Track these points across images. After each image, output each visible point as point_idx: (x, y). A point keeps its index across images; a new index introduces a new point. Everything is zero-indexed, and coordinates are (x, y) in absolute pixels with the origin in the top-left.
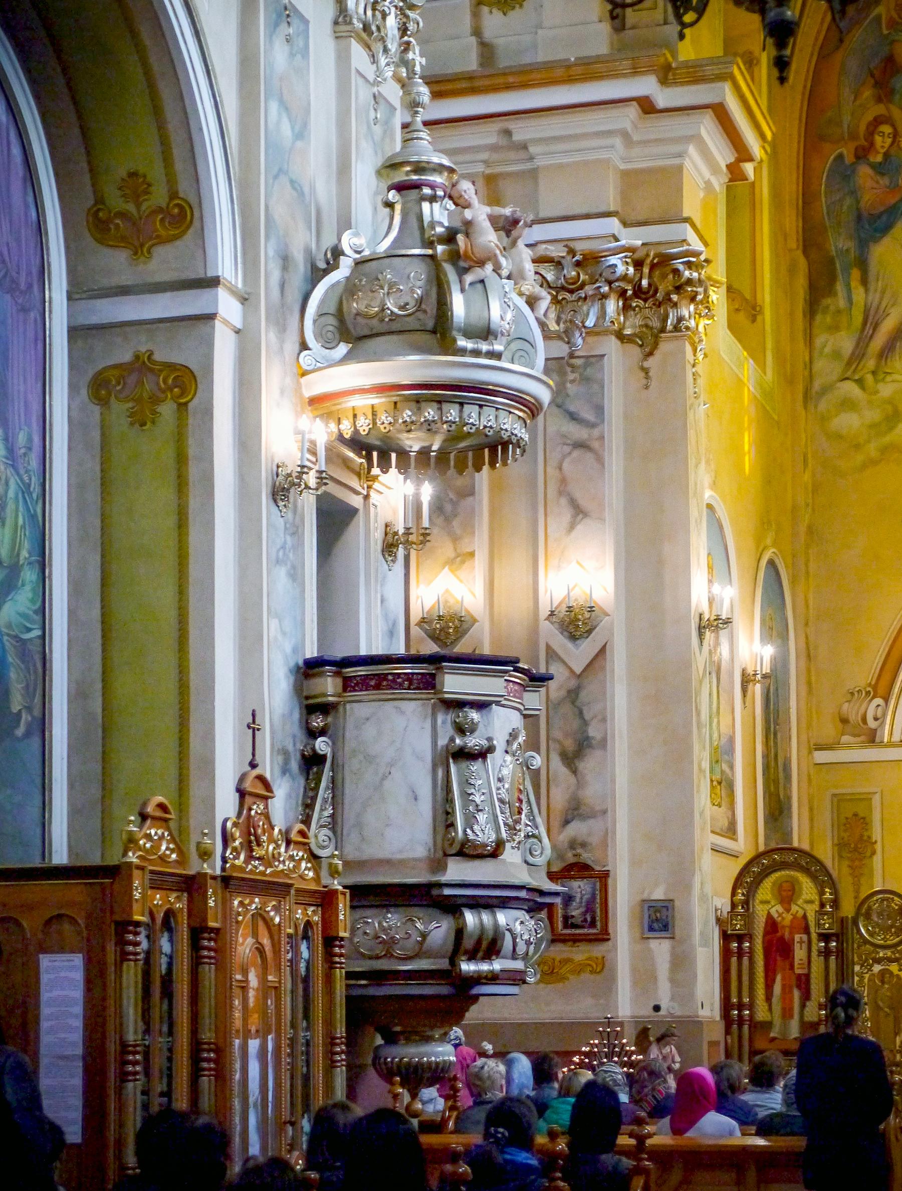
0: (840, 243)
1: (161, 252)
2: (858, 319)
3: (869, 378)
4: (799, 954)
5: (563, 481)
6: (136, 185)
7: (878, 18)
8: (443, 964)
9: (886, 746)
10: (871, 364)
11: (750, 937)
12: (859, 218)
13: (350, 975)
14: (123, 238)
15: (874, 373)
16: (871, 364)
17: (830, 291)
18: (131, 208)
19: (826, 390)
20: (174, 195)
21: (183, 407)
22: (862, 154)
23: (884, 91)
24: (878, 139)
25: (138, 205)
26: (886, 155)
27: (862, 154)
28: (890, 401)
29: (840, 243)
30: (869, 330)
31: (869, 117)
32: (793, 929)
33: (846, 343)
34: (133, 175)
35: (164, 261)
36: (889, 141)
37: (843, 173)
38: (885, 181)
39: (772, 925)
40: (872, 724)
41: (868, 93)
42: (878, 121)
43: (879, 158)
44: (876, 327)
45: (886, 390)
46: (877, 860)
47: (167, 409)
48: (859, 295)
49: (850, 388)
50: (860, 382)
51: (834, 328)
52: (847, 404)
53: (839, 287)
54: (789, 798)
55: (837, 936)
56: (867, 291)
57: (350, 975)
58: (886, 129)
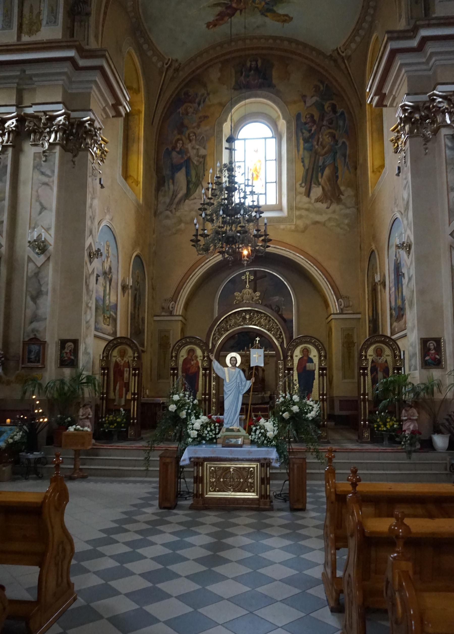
0: (167, 172)
2: (171, 193)
3: (174, 210)
7: (179, 112)
9: (175, 316)
10: (174, 206)
15: (175, 209)
19: (161, 213)
24: (178, 145)
26: (180, 149)
27: (174, 148)
30: (174, 197)
33: (168, 200)
36: (181, 145)
37: (168, 153)
38: (180, 156)
40: (171, 309)
41: (176, 132)
42: (178, 140)
43: (178, 150)
44: (176, 196)
45: (178, 214)
49: (168, 213)
50: (171, 211)
52: (167, 217)
53: (166, 184)
54: (144, 330)
56: (174, 186)
58: (181, 142)
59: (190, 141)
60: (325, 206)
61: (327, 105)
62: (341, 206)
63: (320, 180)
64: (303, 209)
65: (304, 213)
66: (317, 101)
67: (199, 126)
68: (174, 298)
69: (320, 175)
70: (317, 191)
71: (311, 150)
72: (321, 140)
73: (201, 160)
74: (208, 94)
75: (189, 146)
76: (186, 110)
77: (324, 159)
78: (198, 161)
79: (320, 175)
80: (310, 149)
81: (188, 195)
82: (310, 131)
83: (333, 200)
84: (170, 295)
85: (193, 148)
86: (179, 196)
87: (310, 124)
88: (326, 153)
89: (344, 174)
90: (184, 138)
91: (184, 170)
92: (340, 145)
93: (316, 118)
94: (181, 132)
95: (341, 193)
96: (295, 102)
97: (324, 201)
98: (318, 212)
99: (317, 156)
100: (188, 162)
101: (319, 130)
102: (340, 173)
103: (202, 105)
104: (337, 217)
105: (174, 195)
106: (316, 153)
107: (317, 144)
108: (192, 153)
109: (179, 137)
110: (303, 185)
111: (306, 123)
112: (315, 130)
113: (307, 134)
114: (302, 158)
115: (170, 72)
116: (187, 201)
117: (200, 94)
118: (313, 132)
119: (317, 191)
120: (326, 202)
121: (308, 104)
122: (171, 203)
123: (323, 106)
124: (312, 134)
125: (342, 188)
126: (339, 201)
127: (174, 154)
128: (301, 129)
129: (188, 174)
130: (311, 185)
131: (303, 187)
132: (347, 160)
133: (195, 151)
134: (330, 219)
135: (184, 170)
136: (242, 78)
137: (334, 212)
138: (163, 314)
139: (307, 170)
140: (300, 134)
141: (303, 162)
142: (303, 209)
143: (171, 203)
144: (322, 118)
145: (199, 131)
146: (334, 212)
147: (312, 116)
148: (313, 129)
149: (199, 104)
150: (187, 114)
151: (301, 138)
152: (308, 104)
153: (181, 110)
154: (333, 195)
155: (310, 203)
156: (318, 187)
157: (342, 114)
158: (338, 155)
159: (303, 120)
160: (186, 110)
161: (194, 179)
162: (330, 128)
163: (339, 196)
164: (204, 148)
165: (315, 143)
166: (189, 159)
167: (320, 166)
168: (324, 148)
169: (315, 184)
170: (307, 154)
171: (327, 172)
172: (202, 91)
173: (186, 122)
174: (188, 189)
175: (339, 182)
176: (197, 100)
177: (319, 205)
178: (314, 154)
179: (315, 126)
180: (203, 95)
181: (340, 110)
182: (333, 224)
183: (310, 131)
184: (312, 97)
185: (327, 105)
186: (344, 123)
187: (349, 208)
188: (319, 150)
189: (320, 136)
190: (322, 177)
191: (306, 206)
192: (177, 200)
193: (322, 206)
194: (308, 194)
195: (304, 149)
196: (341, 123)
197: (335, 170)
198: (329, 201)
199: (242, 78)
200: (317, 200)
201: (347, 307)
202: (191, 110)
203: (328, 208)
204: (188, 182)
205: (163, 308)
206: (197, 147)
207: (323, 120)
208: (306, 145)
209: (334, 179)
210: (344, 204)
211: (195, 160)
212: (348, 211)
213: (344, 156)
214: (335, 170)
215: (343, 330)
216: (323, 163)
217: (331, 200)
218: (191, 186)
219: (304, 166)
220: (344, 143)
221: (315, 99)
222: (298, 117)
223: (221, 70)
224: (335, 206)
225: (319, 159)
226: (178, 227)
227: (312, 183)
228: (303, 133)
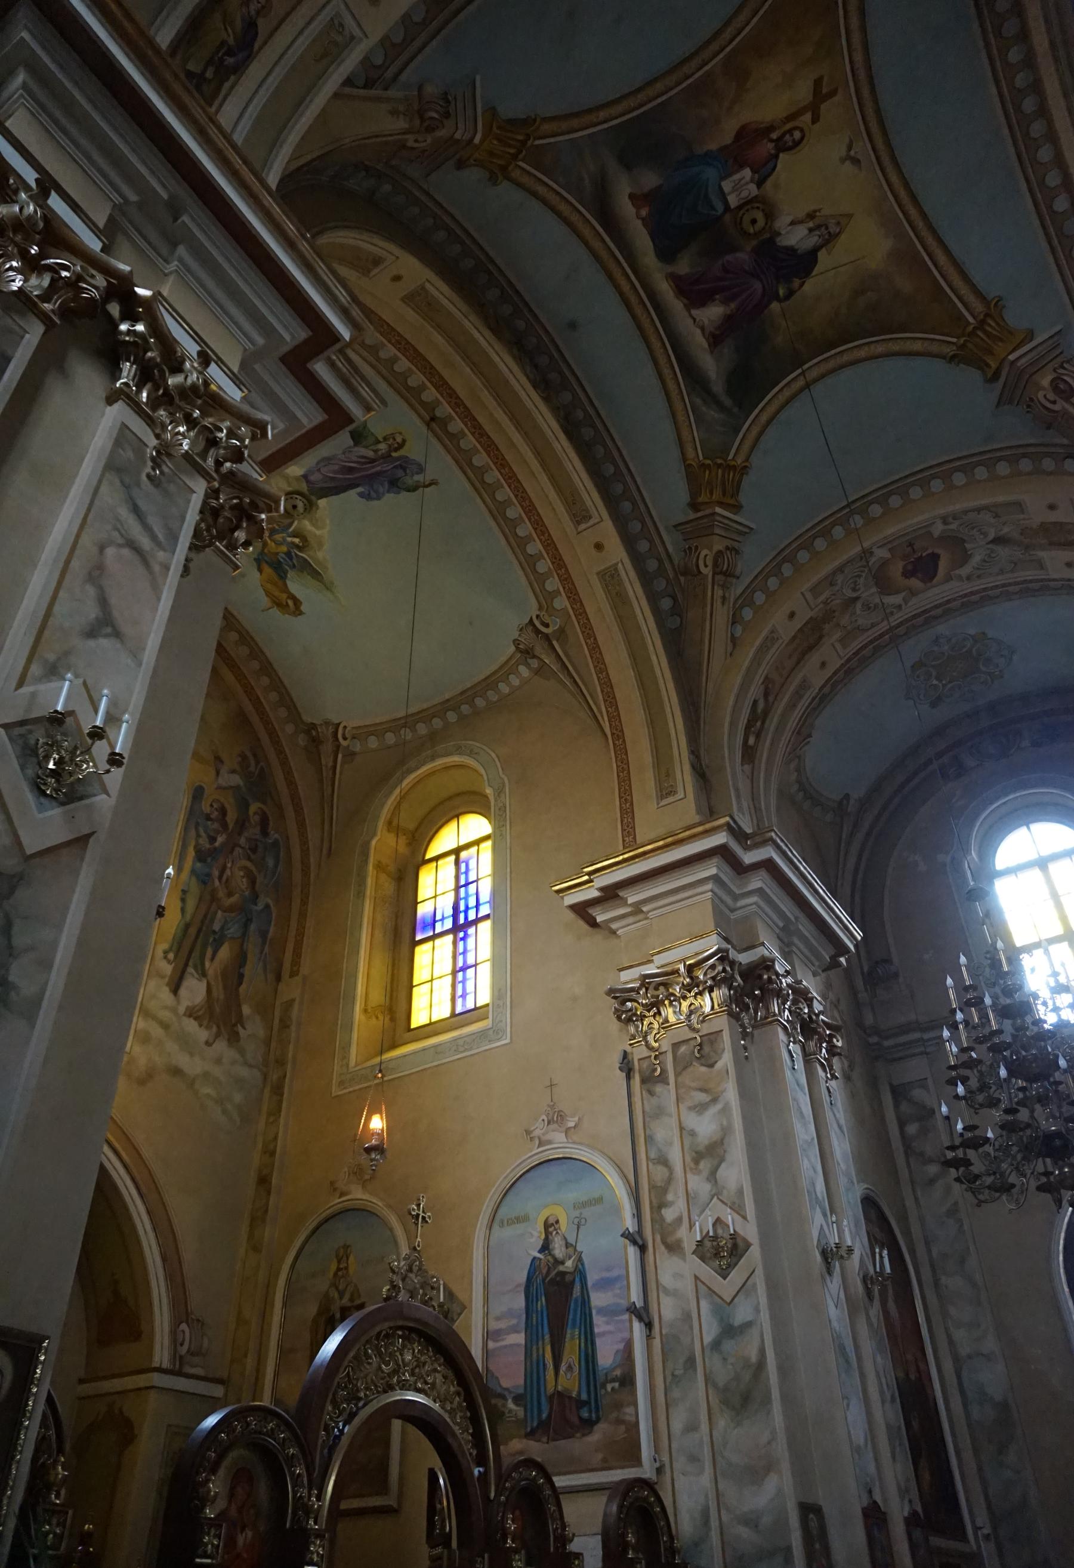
60: (203, 1035)
63: (207, 964)
64: (154, 1018)
65: (157, 1031)
66: (238, 787)
69: (209, 952)
71: (204, 883)
72: (228, 872)
77: (226, 922)
79: (209, 952)
80: (204, 880)
82: (213, 840)
83: (222, 1028)
87: (216, 826)
88: (230, 909)
92: (260, 906)
93: (231, 817)
95: (240, 1020)
97: (205, 1023)
98: (185, 1042)
99: (214, 907)
102: (247, 971)
106: (214, 898)
107: (220, 878)
110: (171, 956)
111: (208, 818)
112: (223, 844)
113: (204, 842)
114: (184, 892)
118: (217, 844)
119: (195, 990)
120: (208, 1028)
121: (221, 781)
124: (215, 849)
125: (246, 1010)
126: (234, 1039)
128: (197, 824)
130: (186, 965)
131: (169, 962)
132: (266, 949)
134: (206, 1075)
137: (218, 1061)
139: (187, 926)
140: (193, 833)
141: (183, 900)
142: (154, 1018)
146: (218, 1061)
147: (223, 811)
148: (220, 840)
151: (193, 843)
152: (221, 781)
154: (222, 1016)
155: (174, 1010)
156: (200, 980)
157: (276, 844)
158: (253, 927)
159: (206, 807)
162: (249, 859)
163: (235, 1025)
165: (216, 873)
167: (214, 932)
168: (230, 895)
169: (195, 968)
170: (195, 888)
171: (225, 952)
175: (242, 989)
179: (224, 836)
181: (274, 836)
182: (207, 1090)
183: (213, 840)
184: (233, 772)
185: (254, 807)
186: (276, 866)
187: (251, 1066)
188: (221, 894)
189: (229, 865)
190: (212, 959)
191: (165, 1015)
195: (193, 871)
196: (270, 862)
197: (241, 959)
198: (215, 1029)
200: (191, 1013)
201: (192, 1354)
203: (208, 1044)
208: (198, 865)
209: (234, 976)
210: (242, 1052)
212: (244, 1072)
213: (264, 934)
214: (241, 959)
216: (222, 928)
217: (218, 1027)
219: (183, 910)
220: (267, 906)
221: (236, 780)
225: (216, 913)
227: (190, 963)
228: (198, 836)
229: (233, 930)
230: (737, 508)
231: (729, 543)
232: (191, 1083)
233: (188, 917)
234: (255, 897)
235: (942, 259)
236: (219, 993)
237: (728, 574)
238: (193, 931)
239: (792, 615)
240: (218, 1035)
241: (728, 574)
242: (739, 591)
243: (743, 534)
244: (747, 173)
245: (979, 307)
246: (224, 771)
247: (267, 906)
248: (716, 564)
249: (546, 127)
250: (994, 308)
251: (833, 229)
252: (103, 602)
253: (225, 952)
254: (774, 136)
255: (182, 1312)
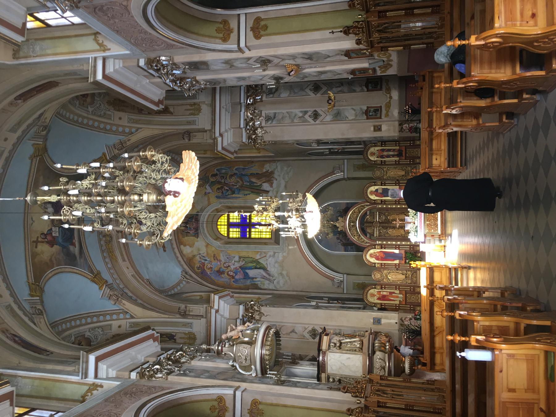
0: (248, 282)
1: (227, 405)
4: (385, 293)
5: (287, 334)
6: (212, 408)
8: (387, 355)
11: (381, 303)
12: (244, 278)
13: (444, 71)
14: (223, 413)
16: (271, 278)
17: (257, 285)
18: (217, 410)
19: (275, 287)
20: (216, 400)
21: (260, 403)
22: (233, 277)
23: (223, 273)
25: (217, 409)
27: (233, 277)
28: (278, 274)
29: (248, 282)
31: (227, 276)
32: (380, 294)
33: (268, 282)
34: (210, 409)
35: (229, 403)
37: (236, 281)
39: (379, 299)
42: (228, 274)
45: (276, 275)
46: (366, 282)
47: (261, 407)
48: (258, 279)
49: (275, 282)
51: (264, 284)
52: (278, 283)
53: (256, 283)
55: (382, 285)
57: (444, 71)
59: (229, 266)
60: (275, 182)
61: (212, 180)
62: (276, 172)
67: (220, 261)
68: (332, 279)
69: (255, 184)
70: (266, 186)
73: (242, 259)
74: (200, 254)
75: (232, 267)
76: (209, 269)
78: (242, 261)
81: (264, 269)
84: (330, 282)
85: (234, 265)
86: (265, 274)
87: (223, 190)
88: (242, 181)
89: (255, 169)
90: (227, 271)
91: (248, 271)
94: (223, 273)
95: (267, 172)
96: (209, 199)
98: (279, 186)
100: (243, 268)
101: (226, 184)
102: (255, 172)
103: (207, 258)
104: (283, 174)
105: (264, 277)
106: (241, 186)
108: (237, 265)
109: (226, 273)
111: (222, 193)
113: (230, 192)
115: (188, 277)
116: (268, 269)
117: (199, 260)
119: (266, 186)
122: (269, 280)
123: (212, 182)
125: (264, 170)
126: (272, 173)
127: (237, 277)
129: (250, 268)
133: (236, 263)
134: (284, 179)
135: (248, 271)
136: (191, 232)
137: (279, 176)
138: (342, 286)
139: (252, 192)
140: (229, 196)
143: (269, 280)
144: (219, 183)
145: (223, 261)
146: (279, 176)
147: (218, 189)
149: (206, 260)
150: (211, 268)
152: (211, 191)
153: (209, 272)
154: (269, 177)
157: (217, 170)
159: (220, 194)
160: (209, 269)
161: (254, 265)
162: (226, 178)
164: (234, 257)
166: (240, 267)
170: (242, 192)
171: (254, 180)
172: (198, 258)
173: (216, 269)
174: (259, 268)
176: (203, 261)
177: (275, 185)
178: (242, 188)
180: (200, 258)
185: (212, 180)
192: (268, 276)
193: (275, 183)
194: (267, 192)
196: (224, 171)
199: (191, 232)
200: (271, 186)
202: (209, 266)
203: (276, 180)
204: (256, 268)
205: (338, 287)
206: (233, 262)
207: (221, 182)
209: (258, 176)
210: (275, 169)
211: (242, 263)
212: (279, 168)
213: (244, 169)
214: (252, 175)
215: (355, 171)
218: (258, 266)
221: (207, 187)
222: (218, 197)
223: (185, 246)
224: (276, 176)
226: (285, 275)
228: (229, 195)
229: (247, 178)
230: (104, 154)
231: (114, 149)
232: (287, 182)
233: (249, 192)
234: (235, 174)
235: (30, 180)
236: (264, 179)
237: (121, 143)
238: (253, 190)
239: (120, 118)
240: (273, 177)
241: (121, 143)
242: (124, 137)
243: (109, 147)
244: (54, 235)
245: (34, 160)
246: (207, 191)
247: (236, 169)
248: (122, 149)
249: (90, 277)
250: (32, 158)
251: (43, 205)
252: (291, 332)
253: (254, 180)
254: (46, 240)
255: (333, 173)
